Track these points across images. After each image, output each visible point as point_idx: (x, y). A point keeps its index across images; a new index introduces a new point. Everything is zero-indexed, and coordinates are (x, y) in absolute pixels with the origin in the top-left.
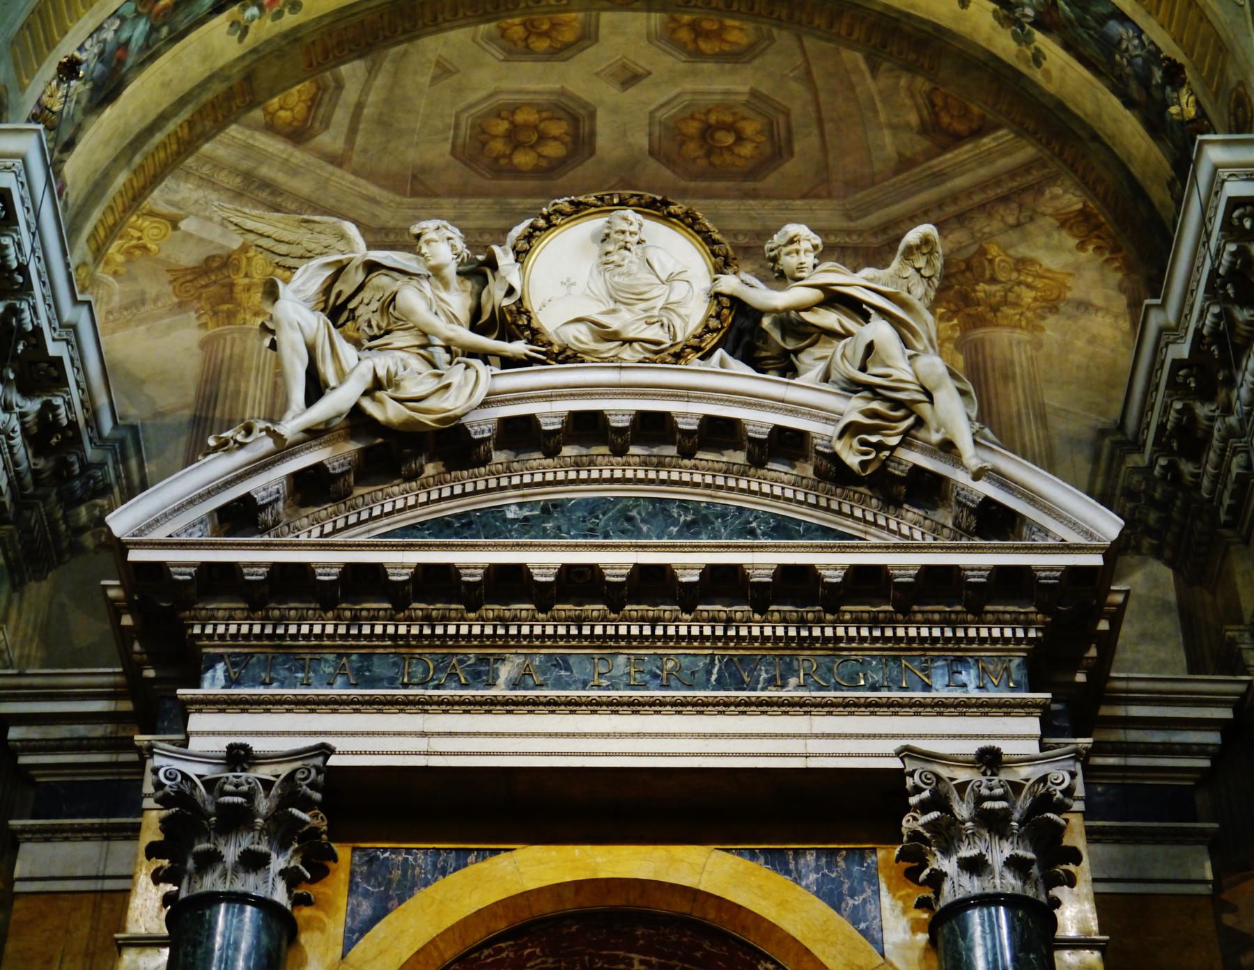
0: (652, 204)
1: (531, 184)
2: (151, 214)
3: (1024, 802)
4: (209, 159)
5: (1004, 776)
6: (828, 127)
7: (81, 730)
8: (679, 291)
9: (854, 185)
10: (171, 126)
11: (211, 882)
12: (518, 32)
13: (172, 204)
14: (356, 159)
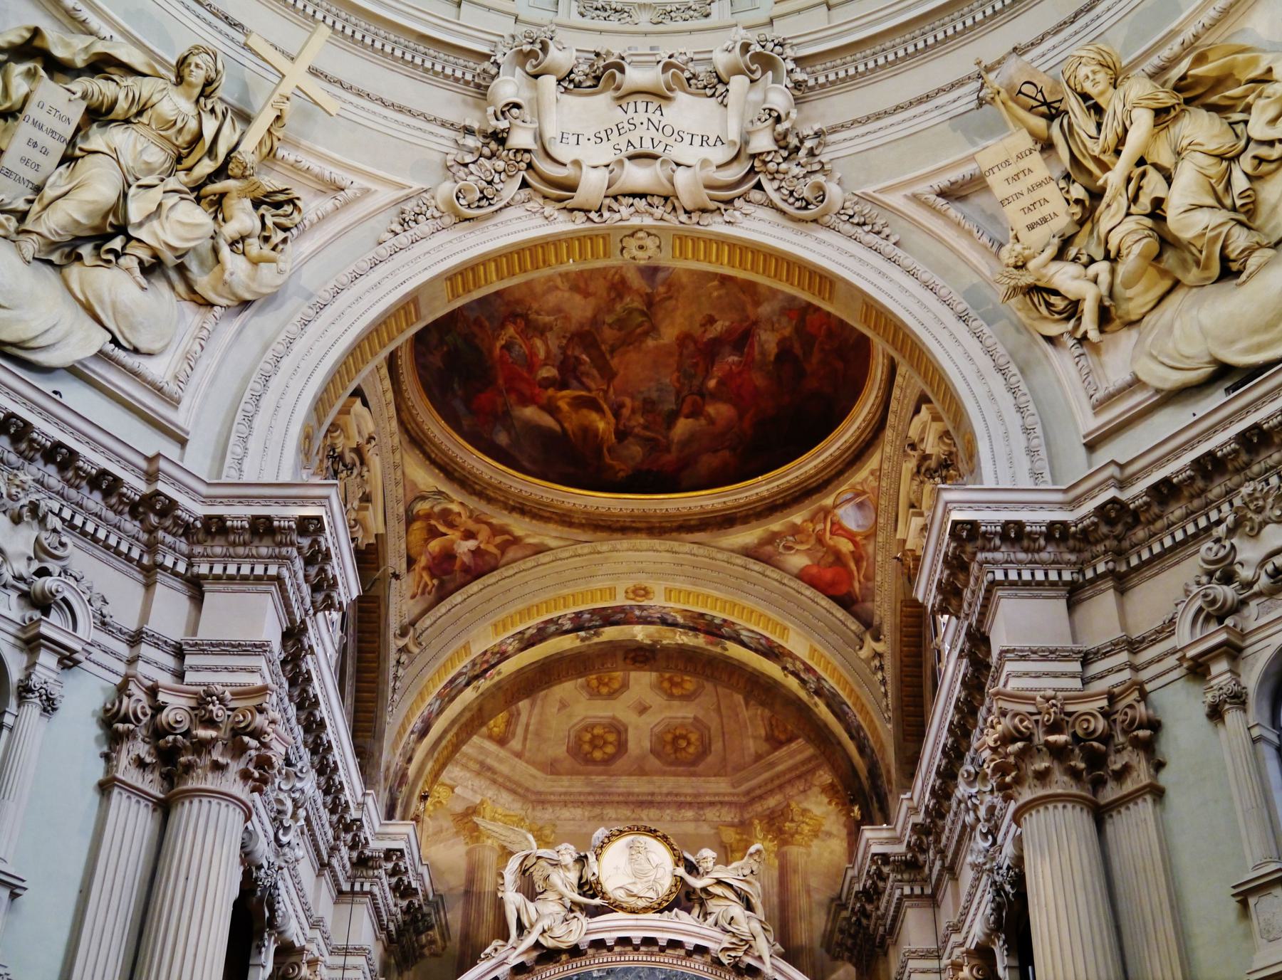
0: (650, 831)
1: (601, 768)
4: (465, 755)
8: (661, 871)
9: (738, 769)
10: (449, 736)
12: (594, 683)
14: (527, 754)
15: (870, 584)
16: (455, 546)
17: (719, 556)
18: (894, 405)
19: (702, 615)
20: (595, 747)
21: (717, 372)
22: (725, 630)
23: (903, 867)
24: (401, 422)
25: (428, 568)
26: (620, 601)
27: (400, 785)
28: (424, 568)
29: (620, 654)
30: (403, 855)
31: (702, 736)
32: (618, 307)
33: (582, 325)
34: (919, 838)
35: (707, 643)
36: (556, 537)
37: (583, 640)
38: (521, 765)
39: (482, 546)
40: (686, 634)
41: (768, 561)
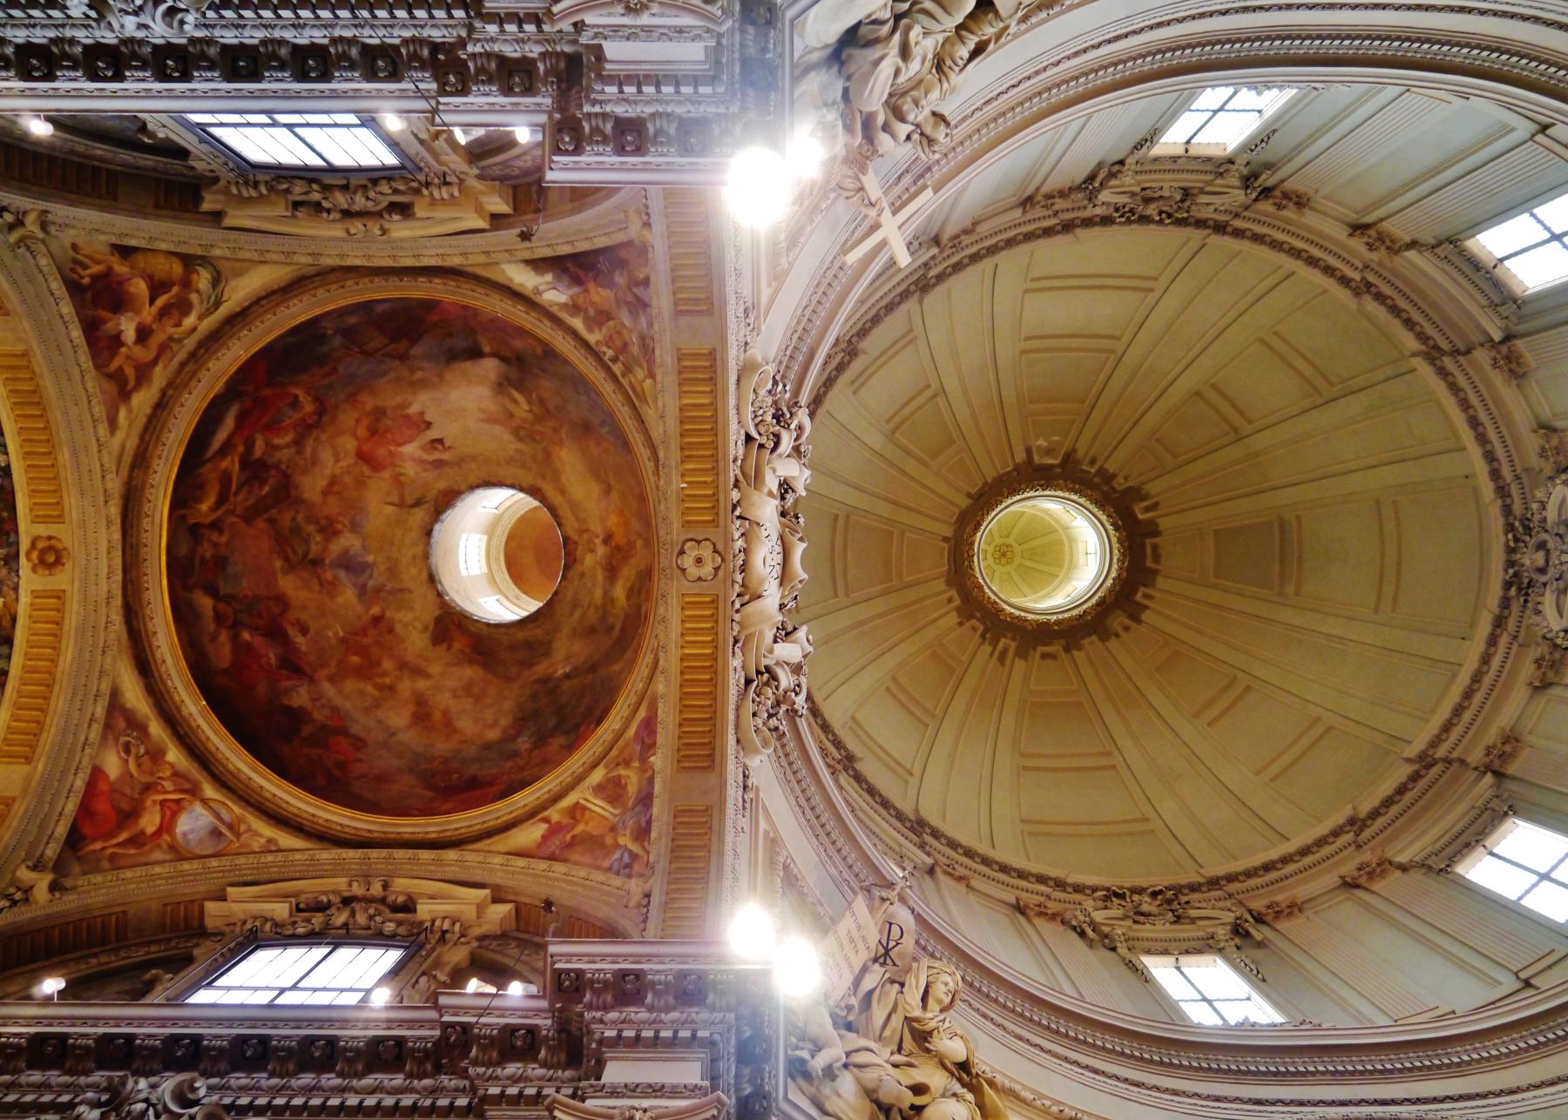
15: (105, 864)
16: (130, 314)
18: (374, 853)
21: (259, 641)
24: (333, 270)
25: (109, 271)
32: (311, 528)
33: (297, 487)
36: (123, 447)
39: (124, 350)
41: (108, 726)
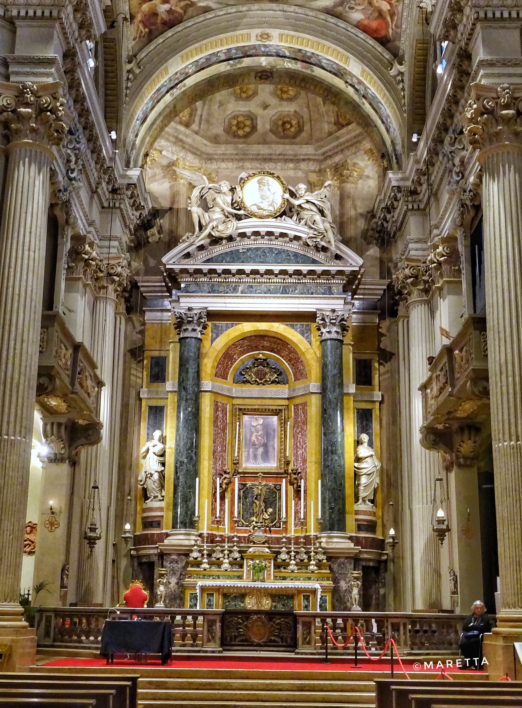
0: (270, 174)
2: (155, 149)
3: (339, 319)
4: (168, 133)
5: (336, 314)
6: (313, 122)
7: (155, 289)
9: (317, 141)
10: (158, 122)
11: (186, 335)
12: (238, 91)
13: (160, 146)
14: (202, 133)
17: (311, 13)
19: (300, 50)
20: (239, 128)
22: (313, 60)
23: (409, 194)
25: (142, 22)
26: (253, 42)
27: (132, 150)
28: (140, 22)
29: (253, 74)
30: (136, 187)
31: (299, 122)
34: (419, 178)
35: (303, 68)
37: (231, 66)
38: (198, 138)
39: (173, 8)
40: (290, 62)
41: (339, 16)
